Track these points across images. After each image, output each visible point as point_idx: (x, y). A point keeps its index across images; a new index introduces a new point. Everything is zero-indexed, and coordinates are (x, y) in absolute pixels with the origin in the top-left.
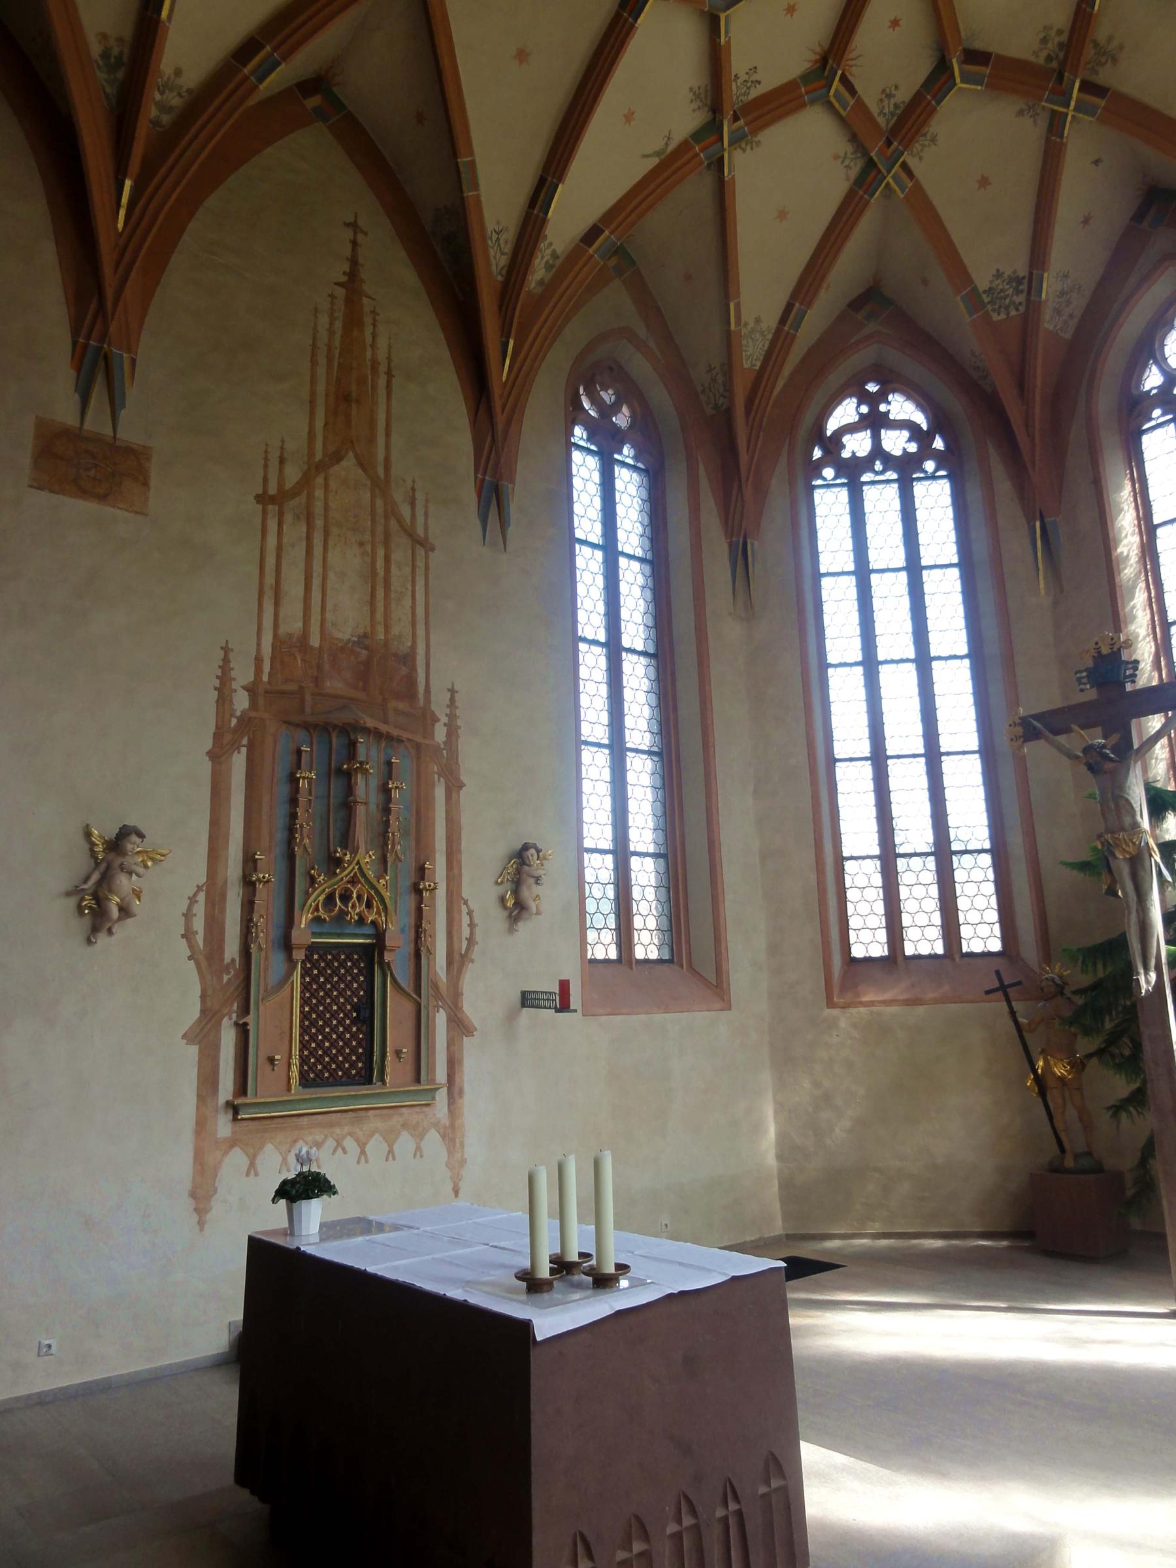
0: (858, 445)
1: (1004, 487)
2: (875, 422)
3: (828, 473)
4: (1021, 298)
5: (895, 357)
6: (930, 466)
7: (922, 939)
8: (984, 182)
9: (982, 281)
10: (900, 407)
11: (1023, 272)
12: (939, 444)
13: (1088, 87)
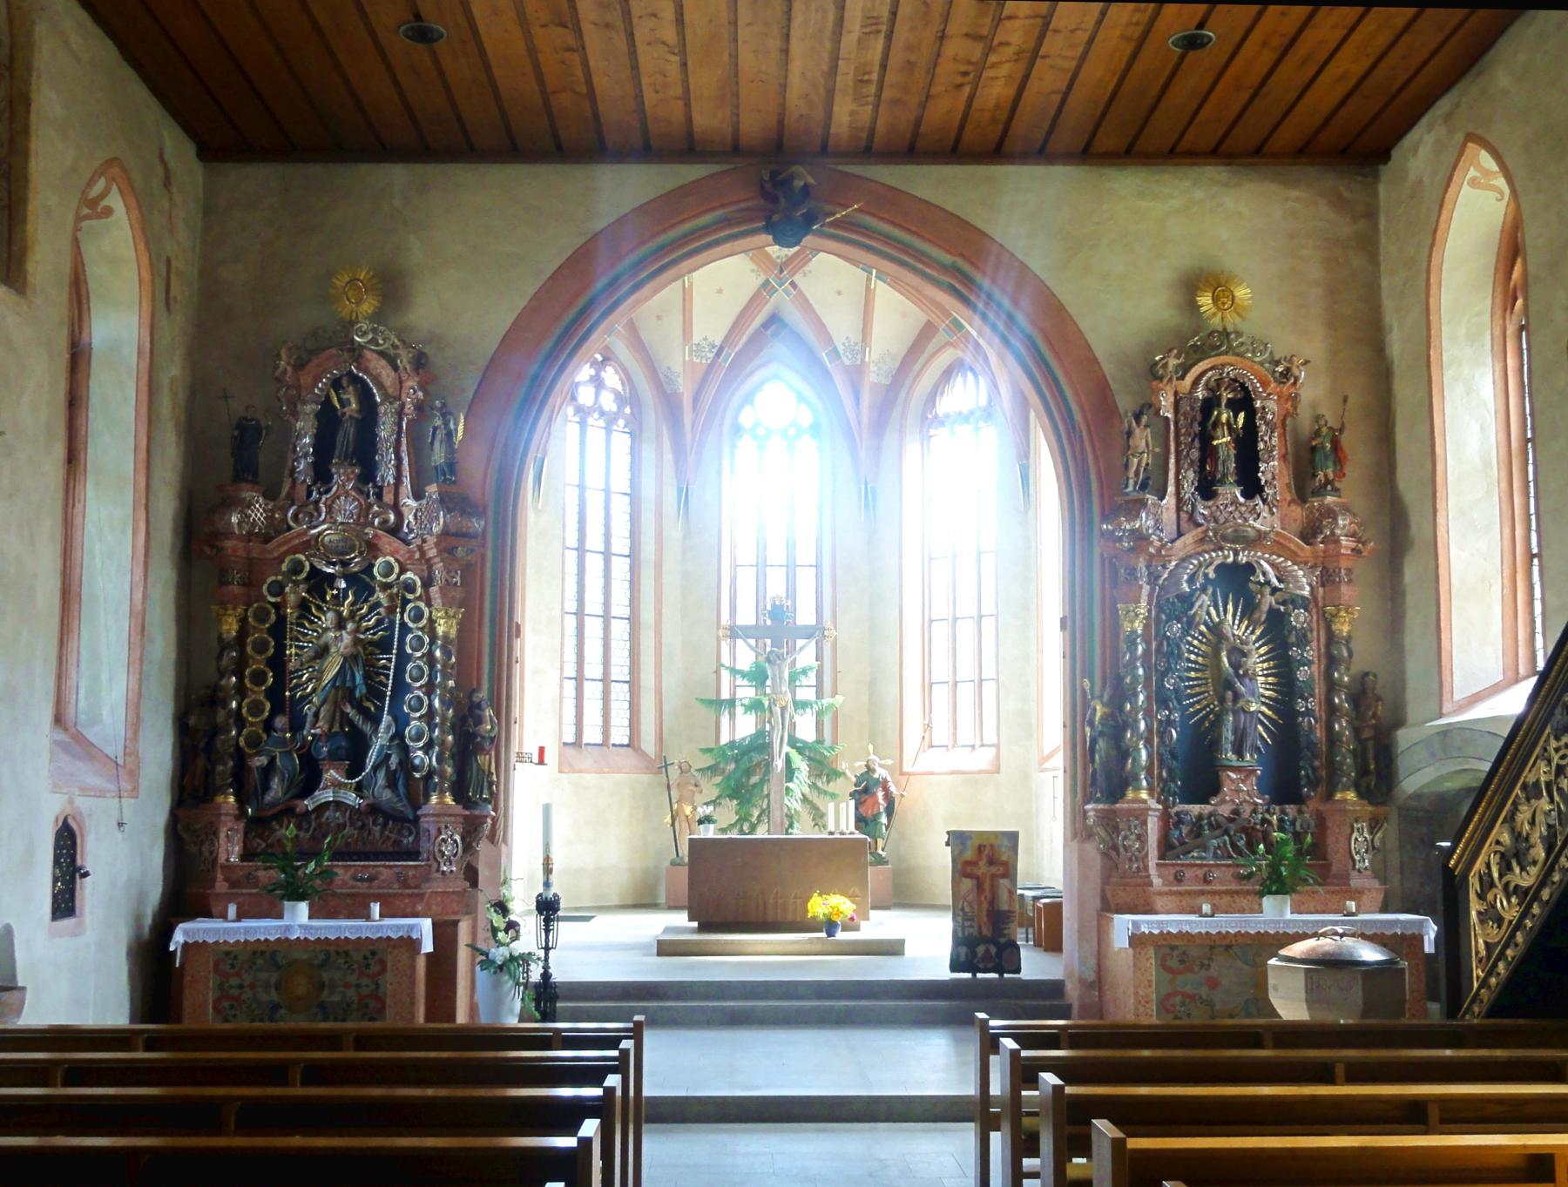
0: (586, 395)
1: (668, 457)
2: (597, 382)
3: (570, 410)
4: (711, 355)
5: (622, 350)
6: (621, 422)
7: (592, 734)
8: (720, 291)
9: (697, 338)
10: (611, 376)
11: (718, 343)
12: (628, 410)
13: (793, 285)
